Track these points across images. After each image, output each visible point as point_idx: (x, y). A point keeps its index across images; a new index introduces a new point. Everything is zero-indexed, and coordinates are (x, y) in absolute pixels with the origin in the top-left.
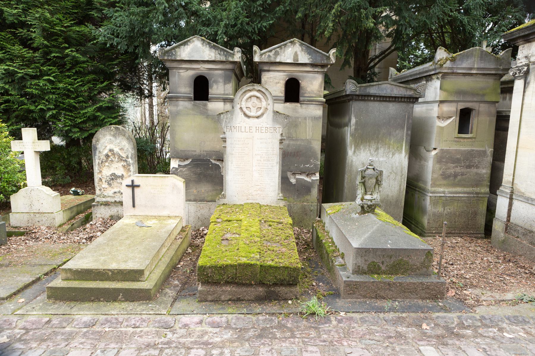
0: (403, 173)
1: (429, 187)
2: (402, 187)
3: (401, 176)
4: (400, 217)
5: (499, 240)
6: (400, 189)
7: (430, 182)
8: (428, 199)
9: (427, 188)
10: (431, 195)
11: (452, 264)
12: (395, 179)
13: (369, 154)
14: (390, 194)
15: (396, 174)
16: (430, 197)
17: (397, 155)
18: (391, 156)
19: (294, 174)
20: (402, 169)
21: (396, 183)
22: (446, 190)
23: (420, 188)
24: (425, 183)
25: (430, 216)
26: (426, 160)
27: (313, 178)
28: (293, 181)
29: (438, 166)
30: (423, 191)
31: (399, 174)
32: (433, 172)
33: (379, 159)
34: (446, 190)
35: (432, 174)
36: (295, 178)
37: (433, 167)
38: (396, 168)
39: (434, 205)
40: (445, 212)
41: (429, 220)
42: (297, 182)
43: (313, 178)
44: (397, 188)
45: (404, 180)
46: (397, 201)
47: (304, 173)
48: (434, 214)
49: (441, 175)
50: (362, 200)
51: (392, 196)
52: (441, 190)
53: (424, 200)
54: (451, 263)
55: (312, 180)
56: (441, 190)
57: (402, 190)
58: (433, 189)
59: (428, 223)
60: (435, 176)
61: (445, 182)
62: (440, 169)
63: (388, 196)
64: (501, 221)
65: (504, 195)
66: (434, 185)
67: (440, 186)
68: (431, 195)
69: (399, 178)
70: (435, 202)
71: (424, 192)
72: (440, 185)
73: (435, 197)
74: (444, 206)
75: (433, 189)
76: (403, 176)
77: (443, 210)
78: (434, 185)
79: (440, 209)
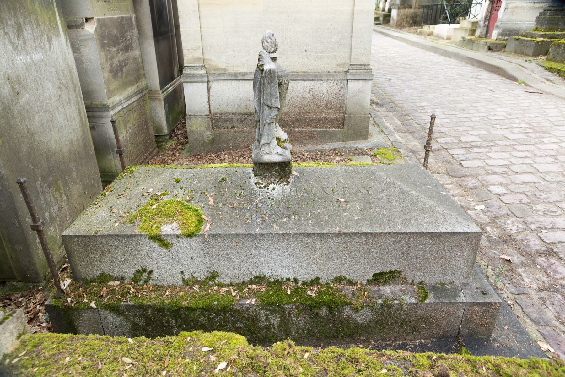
5: (205, 142)
6: (81, 118)
13: (10, 48)
17: (55, 42)
21: (73, 108)
31: (71, 86)
33: (31, 58)
66: (111, 93)
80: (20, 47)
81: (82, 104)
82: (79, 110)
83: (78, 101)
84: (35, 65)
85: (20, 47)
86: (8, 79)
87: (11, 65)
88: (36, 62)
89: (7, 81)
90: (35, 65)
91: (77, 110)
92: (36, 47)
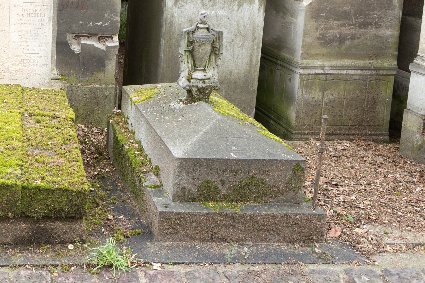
0: (256, 35)
1: (298, 58)
2: (254, 59)
3: (253, 41)
4: (252, 108)
6: (251, 61)
7: (299, 51)
8: (297, 79)
9: (295, 59)
10: (301, 71)
11: (336, 185)
12: (242, 46)
13: (200, 5)
14: (235, 71)
15: (244, 37)
16: (300, 74)
17: (246, 7)
18: (236, 8)
19: (77, 37)
20: (254, 28)
21: (245, 51)
22: (327, 64)
23: (284, 60)
24: (292, 51)
25: (299, 105)
26: (293, 14)
27: (108, 44)
28: (76, 48)
29: (313, 24)
30: (288, 65)
31: (250, 37)
32: (305, 34)
33: (216, 13)
34: (327, 64)
35: (304, 37)
36: (79, 43)
37: (305, 26)
38: (245, 27)
39: (306, 87)
40: (325, 99)
41: (298, 112)
42: (82, 49)
43: (108, 44)
44: (246, 60)
45: (258, 48)
46: (246, 81)
47: (94, 35)
48: (307, 103)
49: (319, 39)
50: (189, 80)
51: (238, 74)
52: (319, 63)
53: (290, 79)
54: (334, 183)
55: (107, 47)
56: (319, 63)
57: (254, 63)
58: (305, 62)
59: (297, 117)
60: (309, 40)
61: (324, 50)
62: (317, 29)
63: (231, 72)
64: (417, 114)
65: (420, 71)
66: (306, 55)
67: (316, 56)
68: (301, 71)
69: (248, 43)
70: (309, 82)
71: (291, 67)
72: (317, 54)
73: (309, 74)
74: (323, 89)
75: (305, 62)
76: (256, 41)
77: (320, 95)
78: (306, 55)
79: (317, 95)
80: (208, 6)
81: (258, 52)
82: (251, 55)
83: (254, 49)
84: (217, 17)
85: (208, 6)
86: (190, 20)
87: (196, 14)
88: (218, 16)
89: (189, 22)
90: (217, 17)
91: (249, 55)
92: (224, 7)
